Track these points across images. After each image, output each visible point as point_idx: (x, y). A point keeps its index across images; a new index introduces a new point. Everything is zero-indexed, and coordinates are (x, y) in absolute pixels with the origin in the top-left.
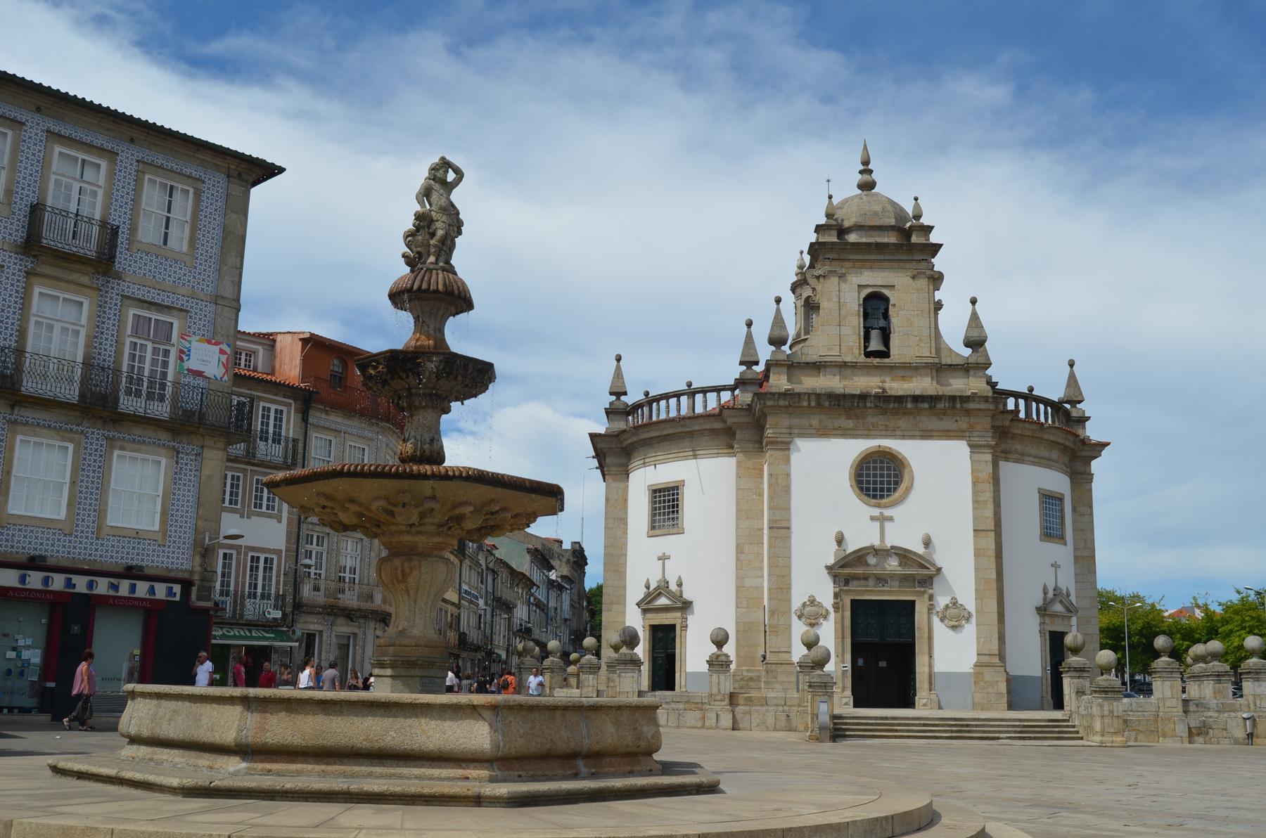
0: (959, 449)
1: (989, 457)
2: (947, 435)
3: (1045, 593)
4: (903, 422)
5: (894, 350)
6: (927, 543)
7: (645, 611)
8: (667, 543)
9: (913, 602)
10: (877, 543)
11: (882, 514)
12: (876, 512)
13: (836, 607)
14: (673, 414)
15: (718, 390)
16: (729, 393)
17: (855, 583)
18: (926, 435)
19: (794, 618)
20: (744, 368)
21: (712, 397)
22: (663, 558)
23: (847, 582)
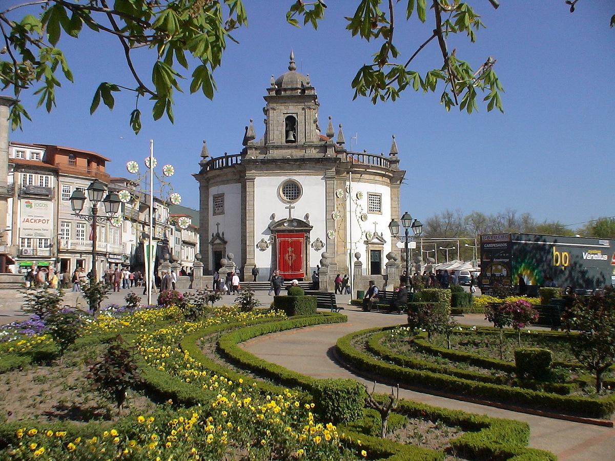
2: (318, 175)
6: (307, 217)
7: (212, 245)
8: (219, 218)
10: (288, 218)
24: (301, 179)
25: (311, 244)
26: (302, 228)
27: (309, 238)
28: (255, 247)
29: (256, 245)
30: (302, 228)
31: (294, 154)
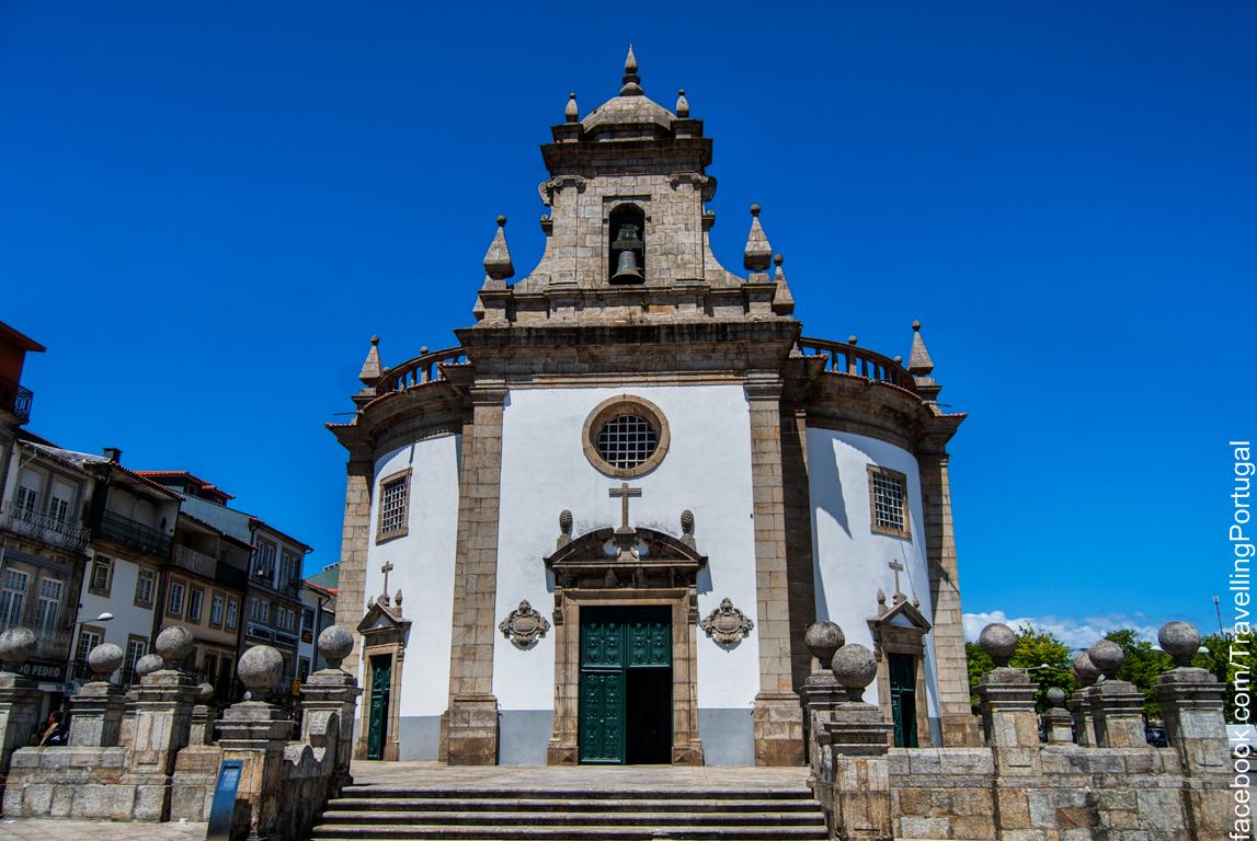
0: (733, 394)
1: (775, 405)
3: (882, 602)
5: (647, 277)
6: (688, 524)
9: (669, 608)
10: (617, 526)
11: (625, 486)
12: (618, 484)
13: (559, 619)
17: (586, 582)
19: (499, 634)
22: (387, 569)
24: (664, 397)
26: (675, 563)
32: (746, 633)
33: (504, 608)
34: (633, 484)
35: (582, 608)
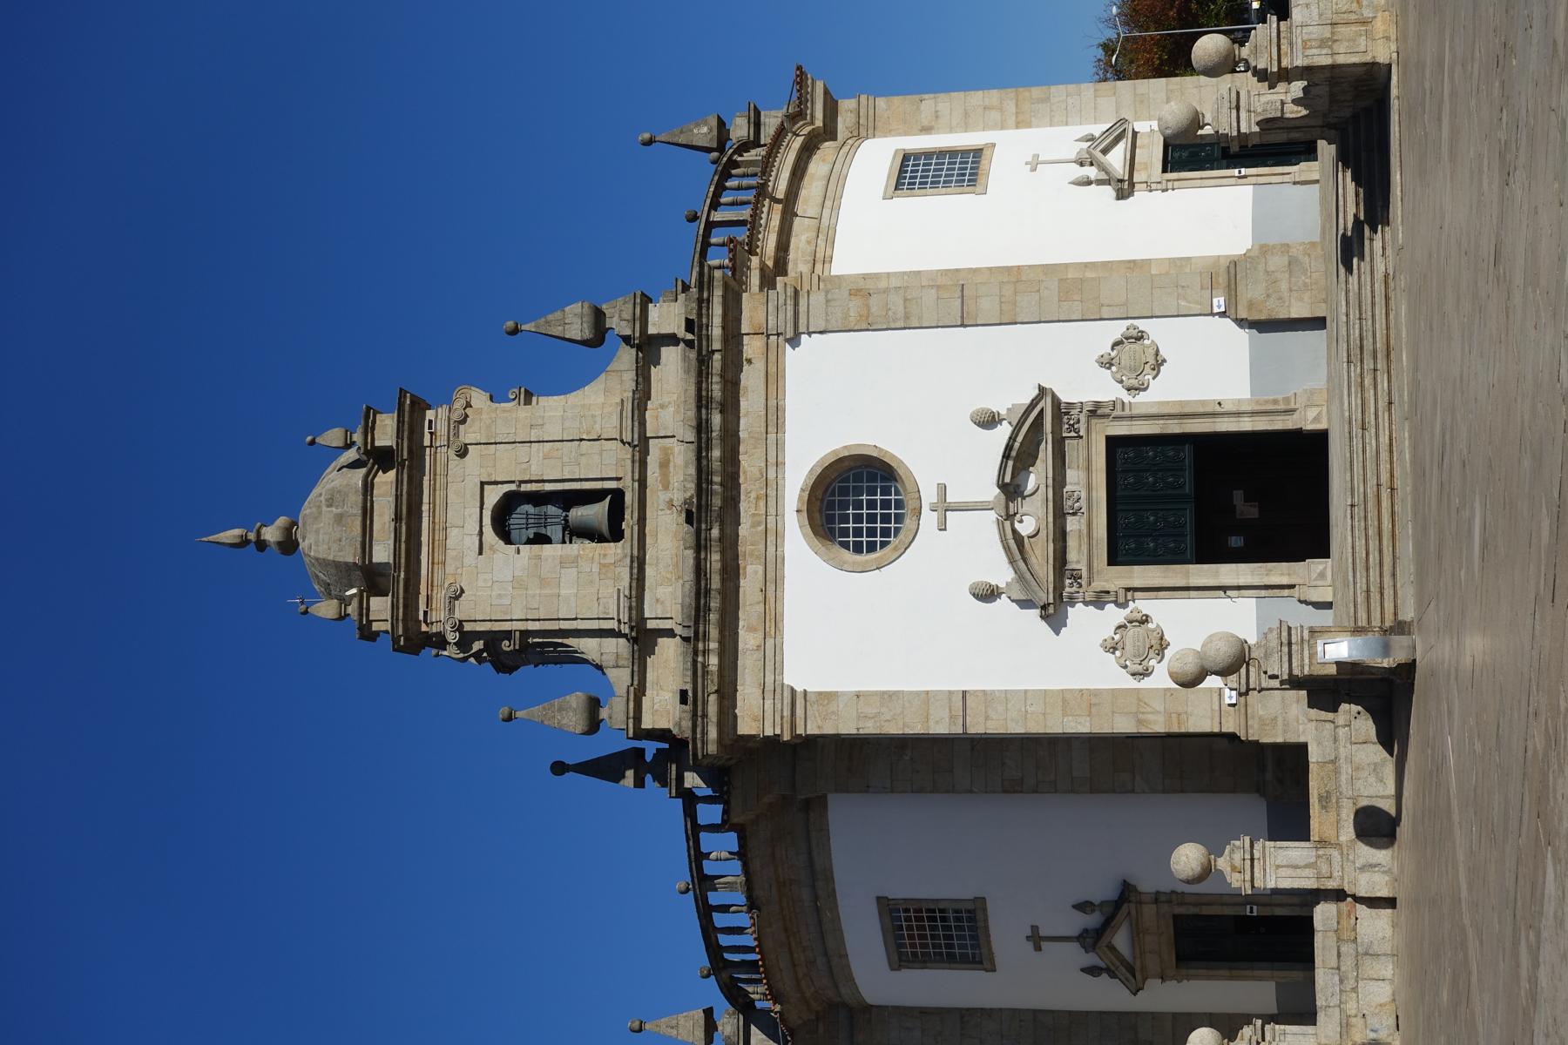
4: (750, 463)
10: (992, 516)
12: (929, 519)
14: (743, 920)
15: (694, 830)
16: (700, 807)
18: (774, 418)
20: (648, 778)
21: (707, 841)
23: (1076, 577)
25: (1126, 397)
27: (1098, 405)
28: (1146, 683)
29: (1132, 683)
30: (1038, 433)
31: (678, 497)
32: (1140, 337)
33: (1110, 675)
34: (929, 496)
35: (1112, 561)
